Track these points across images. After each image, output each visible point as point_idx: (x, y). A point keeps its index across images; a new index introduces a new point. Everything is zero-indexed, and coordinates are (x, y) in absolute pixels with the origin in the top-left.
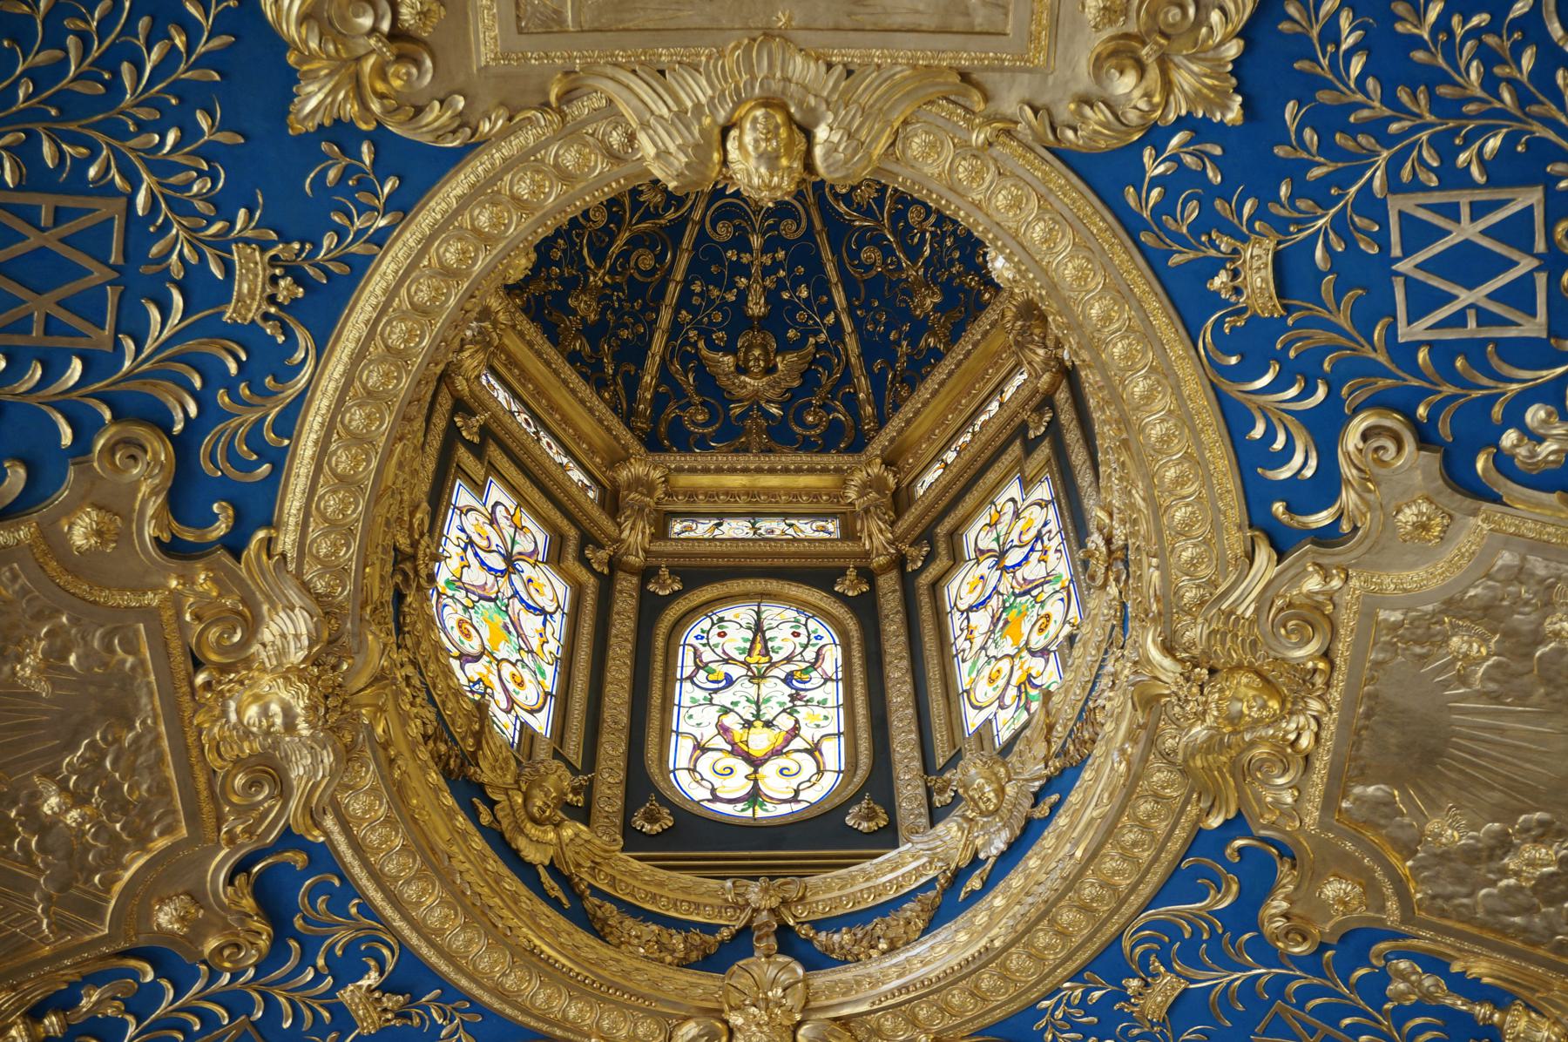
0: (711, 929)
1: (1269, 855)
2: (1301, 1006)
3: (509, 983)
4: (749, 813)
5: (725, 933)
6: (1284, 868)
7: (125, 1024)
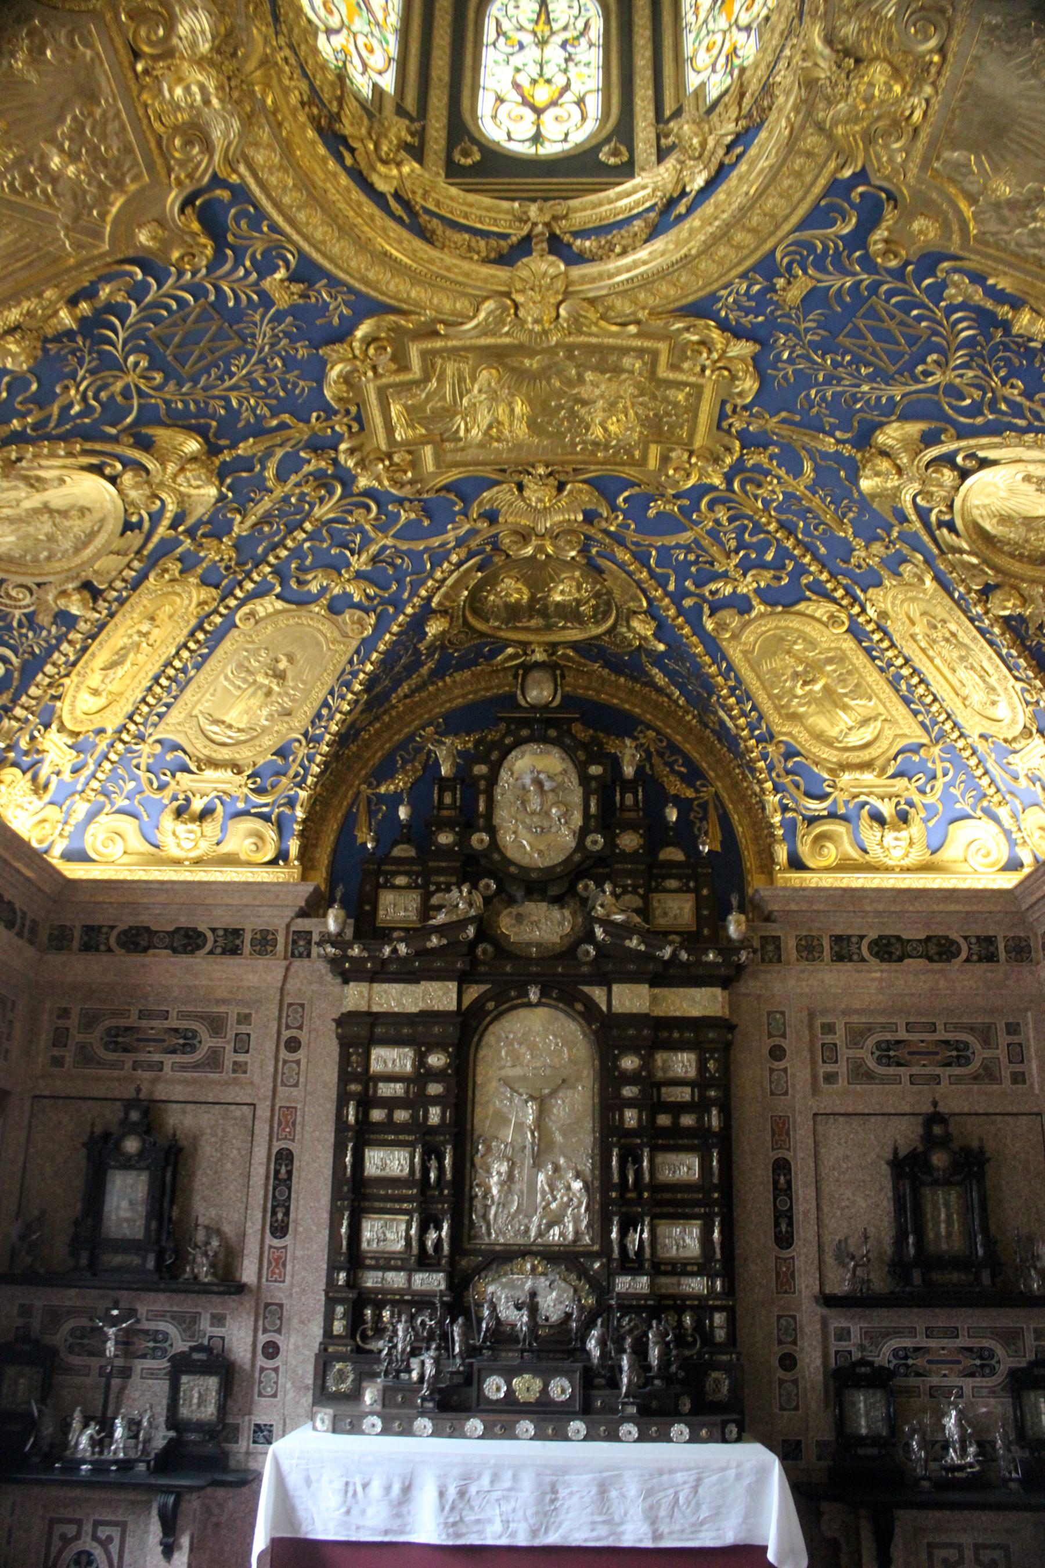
0: (505, 236)
1: (880, 199)
2: (887, 301)
3: (371, 275)
4: (532, 151)
5: (514, 239)
6: (888, 208)
7: (129, 307)
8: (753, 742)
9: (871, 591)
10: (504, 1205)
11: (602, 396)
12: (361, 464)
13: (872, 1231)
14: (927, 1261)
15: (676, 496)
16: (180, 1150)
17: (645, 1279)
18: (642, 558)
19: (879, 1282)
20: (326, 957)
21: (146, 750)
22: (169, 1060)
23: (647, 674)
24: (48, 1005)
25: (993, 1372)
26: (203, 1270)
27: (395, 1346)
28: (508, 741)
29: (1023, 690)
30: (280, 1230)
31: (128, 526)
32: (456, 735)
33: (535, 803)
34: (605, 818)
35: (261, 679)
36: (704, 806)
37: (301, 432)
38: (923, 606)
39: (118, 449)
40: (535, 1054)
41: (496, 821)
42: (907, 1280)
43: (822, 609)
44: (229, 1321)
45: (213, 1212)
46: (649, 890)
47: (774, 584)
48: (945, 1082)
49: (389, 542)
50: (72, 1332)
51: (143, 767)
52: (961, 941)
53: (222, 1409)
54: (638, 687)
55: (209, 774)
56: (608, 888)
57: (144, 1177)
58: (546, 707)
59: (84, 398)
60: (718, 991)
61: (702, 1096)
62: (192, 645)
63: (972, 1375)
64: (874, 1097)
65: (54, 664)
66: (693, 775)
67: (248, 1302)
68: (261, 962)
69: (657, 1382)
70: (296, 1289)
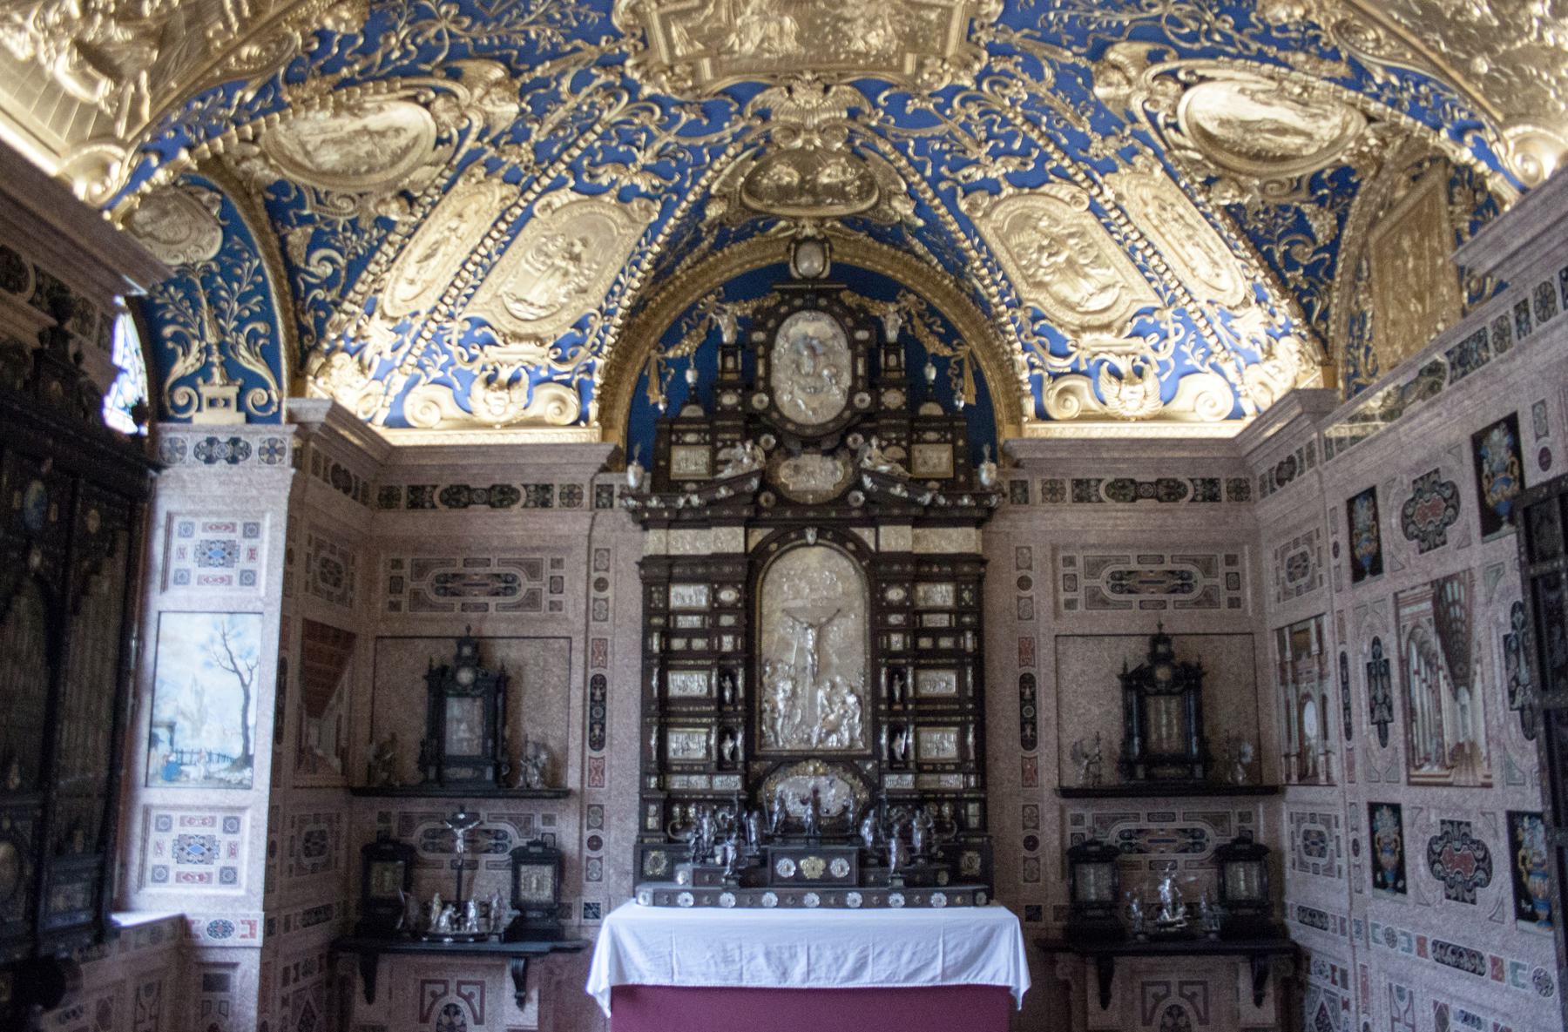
8: (1003, 308)
9: (1108, 177)
10: (789, 716)
11: (862, 15)
12: (647, 75)
13: (1103, 734)
14: (1151, 759)
15: (932, 95)
16: (508, 679)
17: (910, 777)
18: (901, 148)
19: (1110, 775)
20: (628, 508)
21: (456, 329)
22: (493, 602)
23: (908, 243)
24: (383, 556)
25: (1202, 850)
26: (534, 778)
27: (701, 837)
28: (783, 310)
29: (1243, 267)
30: (598, 743)
31: (440, 141)
32: (735, 301)
33: (807, 366)
34: (873, 380)
35: (559, 262)
36: (960, 363)
37: (591, 52)
38: (1154, 192)
39: (432, 82)
40: (813, 589)
41: (774, 383)
42: (1132, 775)
43: (1064, 190)
44: (558, 820)
45: (539, 730)
46: (911, 442)
47: (1022, 169)
48: (1170, 607)
49: (671, 139)
50: (426, 834)
51: (455, 342)
52: (1188, 483)
53: (557, 891)
54: (900, 254)
55: (514, 346)
56: (874, 442)
57: (479, 702)
58: (815, 279)
59: (403, 44)
60: (972, 531)
61: (958, 621)
62: (495, 234)
63: (1185, 851)
64: (1108, 620)
65: (377, 263)
66: (950, 335)
67: (574, 804)
68: (569, 514)
69: (920, 861)
70: (614, 792)
